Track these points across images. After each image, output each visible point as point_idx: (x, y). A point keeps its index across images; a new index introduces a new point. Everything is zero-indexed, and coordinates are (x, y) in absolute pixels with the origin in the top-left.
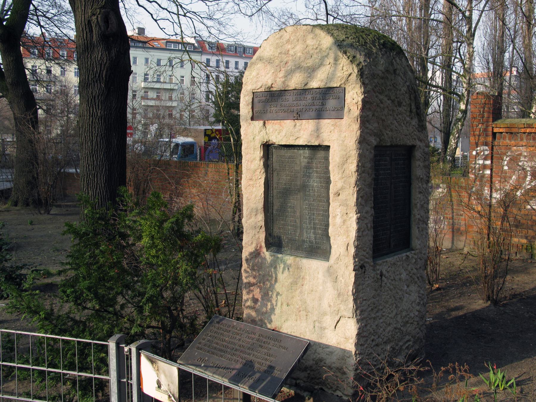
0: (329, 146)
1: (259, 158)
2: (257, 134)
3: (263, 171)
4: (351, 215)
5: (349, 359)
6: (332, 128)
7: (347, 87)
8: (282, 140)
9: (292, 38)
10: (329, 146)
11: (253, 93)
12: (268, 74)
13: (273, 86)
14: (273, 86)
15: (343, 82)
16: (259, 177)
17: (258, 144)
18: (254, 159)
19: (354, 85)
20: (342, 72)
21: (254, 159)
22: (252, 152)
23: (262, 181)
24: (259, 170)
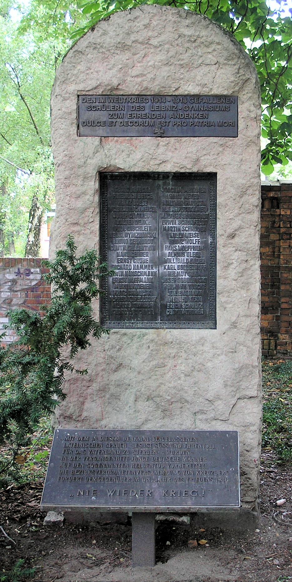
0: (215, 174)
1: (93, 192)
2: (91, 155)
3: (97, 210)
4: (252, 262)
5: (249, 453)
6: (221, 149)
7: (240, 96)
8: (135, 165)
9: (154, 23)
10: (215, 174)
11: (78, 96)
12: (110, 69)
13: (120, 87)
14: (120, 87)
15: (237, 88)
16: (91, 220)
17: (92, 172)
18: (84, 193)
19: (250, 95)
20: (17, 42)
21: (84, 193)
22: (80, 182)
23: (96, 226)
24: (91, 210)
